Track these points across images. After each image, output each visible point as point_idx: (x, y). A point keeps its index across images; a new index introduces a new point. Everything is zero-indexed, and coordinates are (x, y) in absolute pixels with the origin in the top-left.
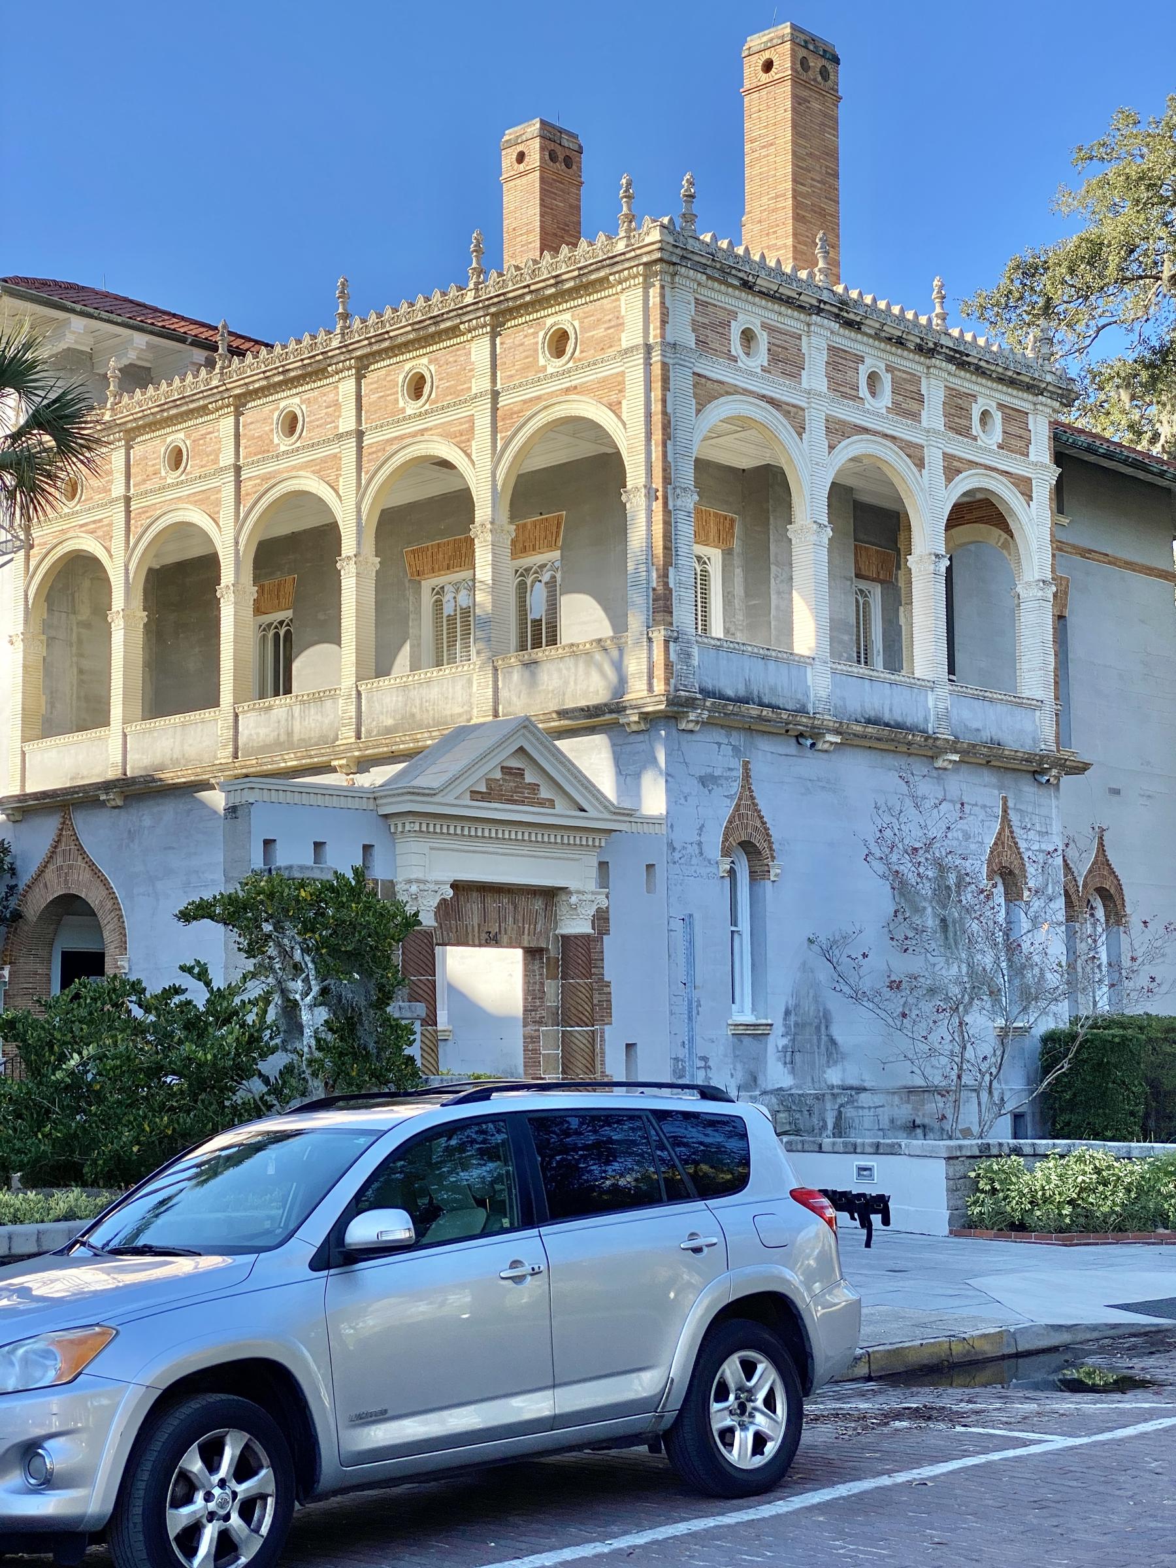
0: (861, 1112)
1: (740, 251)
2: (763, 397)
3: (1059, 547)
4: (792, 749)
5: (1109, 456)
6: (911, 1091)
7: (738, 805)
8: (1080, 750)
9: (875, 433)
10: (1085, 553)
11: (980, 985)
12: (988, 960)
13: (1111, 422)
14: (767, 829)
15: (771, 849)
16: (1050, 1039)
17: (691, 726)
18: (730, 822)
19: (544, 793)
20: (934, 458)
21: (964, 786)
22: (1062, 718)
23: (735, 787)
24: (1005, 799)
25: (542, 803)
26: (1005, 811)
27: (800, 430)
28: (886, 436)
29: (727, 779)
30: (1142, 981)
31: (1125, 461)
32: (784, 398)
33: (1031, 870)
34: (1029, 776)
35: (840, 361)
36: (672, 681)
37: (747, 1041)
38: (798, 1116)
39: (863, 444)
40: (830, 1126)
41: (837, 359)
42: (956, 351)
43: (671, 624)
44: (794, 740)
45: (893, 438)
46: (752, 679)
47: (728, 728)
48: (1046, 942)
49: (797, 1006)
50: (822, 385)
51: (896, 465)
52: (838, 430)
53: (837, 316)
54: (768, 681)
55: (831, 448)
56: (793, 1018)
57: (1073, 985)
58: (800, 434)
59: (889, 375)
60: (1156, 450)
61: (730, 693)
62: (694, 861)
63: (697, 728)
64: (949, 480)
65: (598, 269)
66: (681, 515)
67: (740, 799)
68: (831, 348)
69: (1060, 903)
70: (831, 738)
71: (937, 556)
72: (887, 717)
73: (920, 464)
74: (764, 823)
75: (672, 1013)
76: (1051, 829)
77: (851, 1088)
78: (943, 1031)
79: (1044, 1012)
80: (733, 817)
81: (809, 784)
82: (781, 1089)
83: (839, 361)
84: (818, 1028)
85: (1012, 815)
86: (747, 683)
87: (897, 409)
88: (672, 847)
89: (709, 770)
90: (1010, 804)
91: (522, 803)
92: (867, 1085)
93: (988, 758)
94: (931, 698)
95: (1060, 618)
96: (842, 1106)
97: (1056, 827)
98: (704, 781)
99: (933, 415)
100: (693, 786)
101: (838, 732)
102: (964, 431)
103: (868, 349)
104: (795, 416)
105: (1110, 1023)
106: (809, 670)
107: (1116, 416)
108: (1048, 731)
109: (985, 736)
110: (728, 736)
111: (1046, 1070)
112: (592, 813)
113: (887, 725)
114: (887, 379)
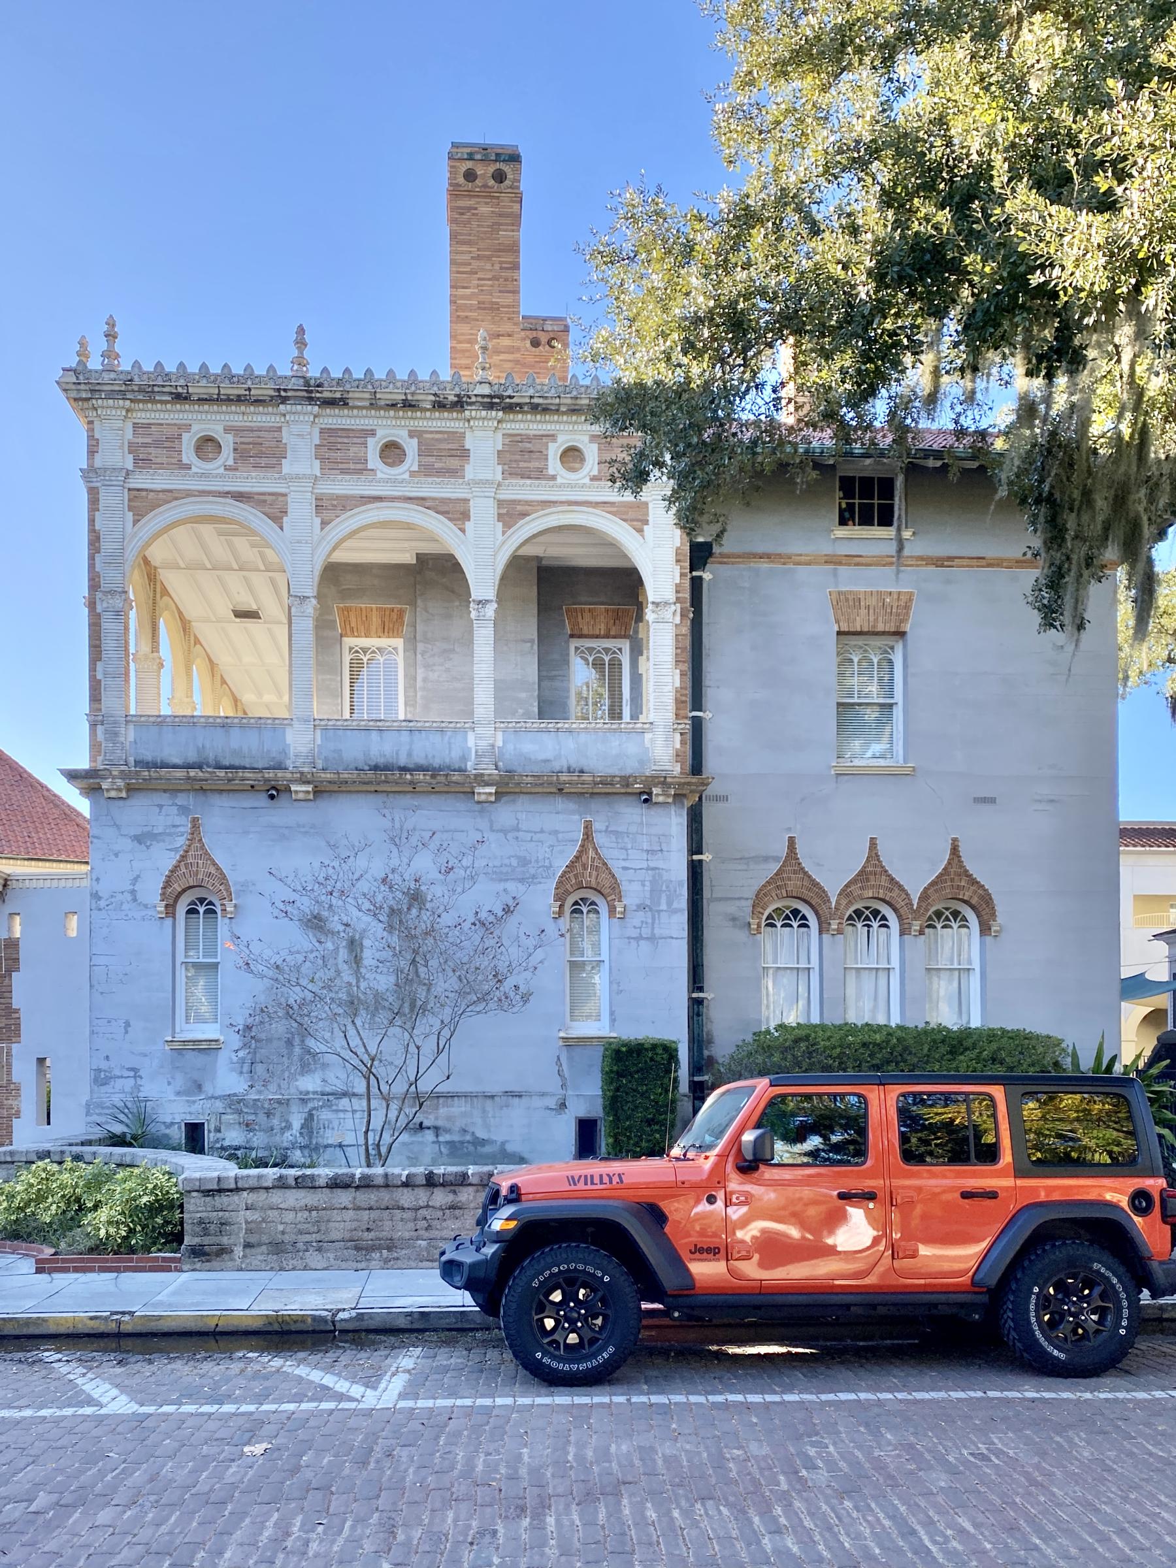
14: (222, 873)
17: (113, 794)
23: (181, 841)
29: (170, 834)
35: (340, 440)
39: (375, 513)
41: (332, 440)
46: (208, 745)
47: (174, 791)
55: (324, 523)
63: (124, 795)
74: (218, 869)
80: (176, 867)
84: (289, 1043)
89: (149, 828)
100: (128, 844)
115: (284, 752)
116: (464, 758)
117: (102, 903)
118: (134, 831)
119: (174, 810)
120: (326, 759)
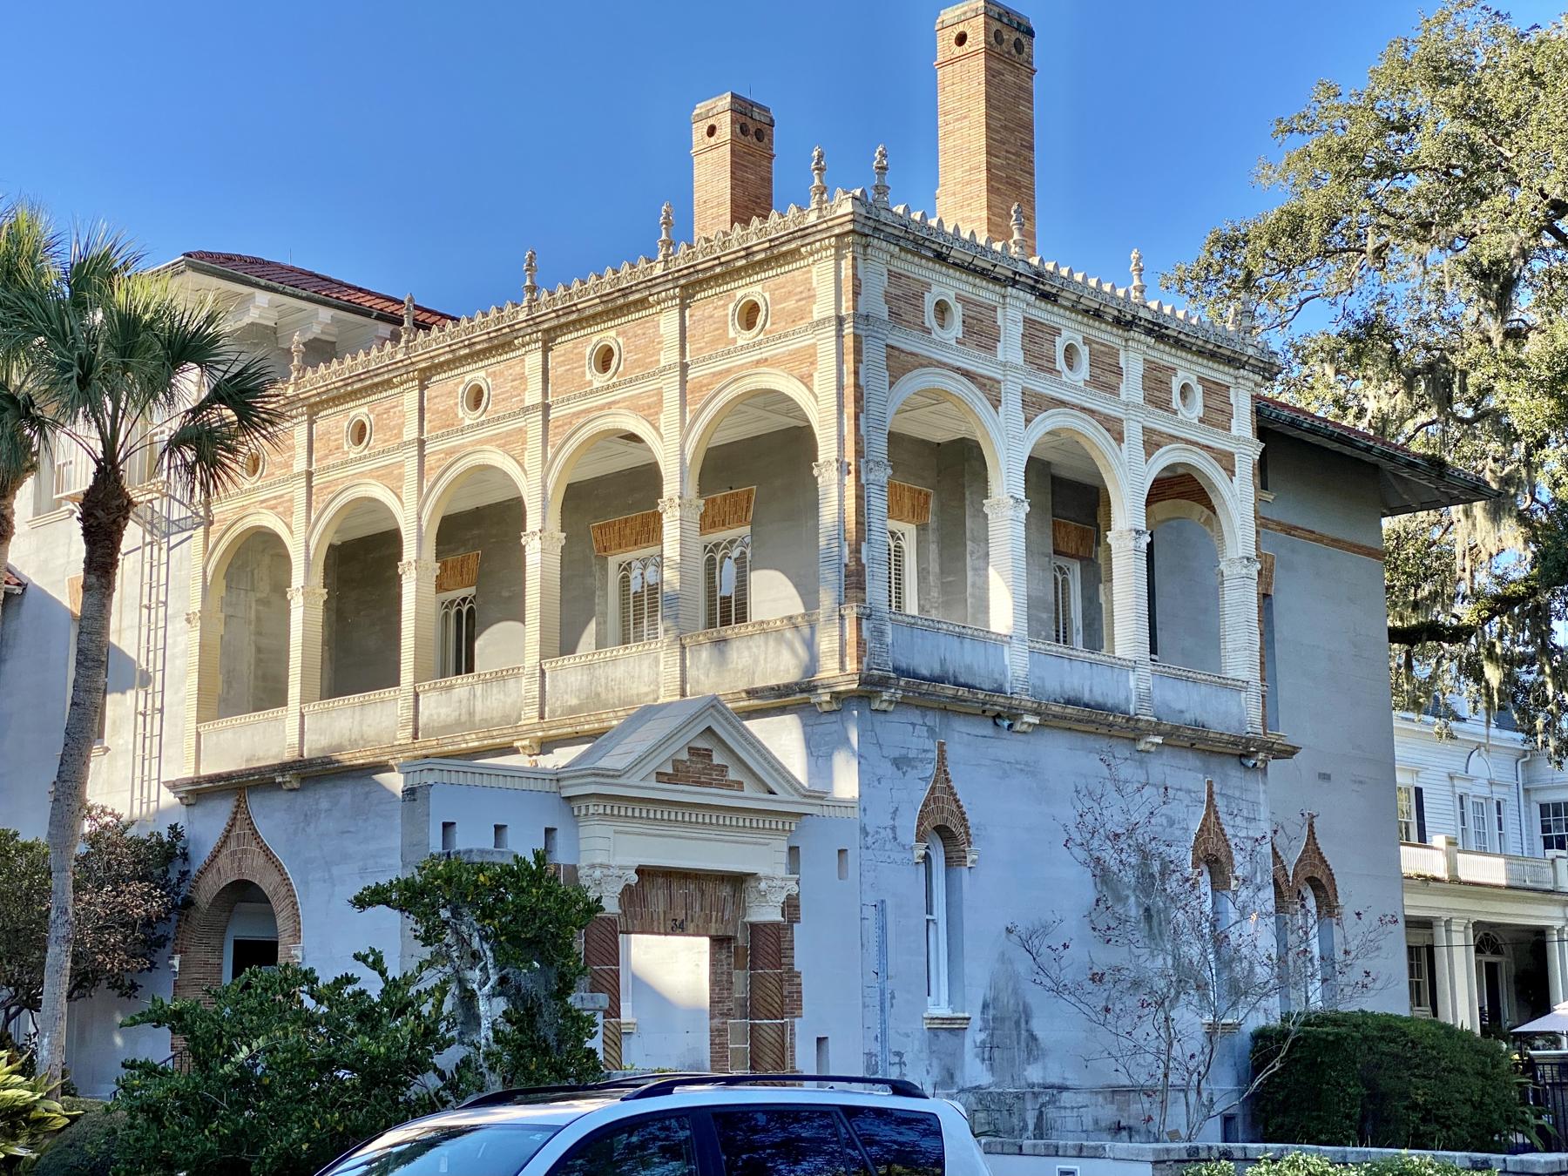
0: (1063, 1113)
1: (933, 222)
2: (958, 370)
3: (1262, 523)
4: (988, 730)
5: (1313, 430)
6: (1115, 1091)
7: (933, 789)
8: (1286, 734)
9: (1073, 406)
10: (1289, 530)
11: (1185, 978)
12: (1193, 952)
13: (1316, 394)
15: (967, 833)
16: (1261, 1036)
17: (884, 706)
18: (925, 805)
19: (732, 775)
20: (1133, 432)
21: (1168, 770)
22: (1268, 701)
23: (930, 770)
24: (1210, 784)
25: (730, 785)
26: (1210, 795)
27: (996, 403)
28: (1083, 409)
30: (1356, 975)
31: (1331, 436)
32: (980, 371)
33: (1238, 858)
34: (1235, 760)
36: (865, 660)
37: (943, 1035)
38: (997, 1115)
39: (1060, 418)
40: (1031, 1127)
42: (1154, 324)
43: (864, 601)
44: (991, 722)
45: (1092, 412)
47: (924, 709)
48: (1255, 934)
49: (995, 999)
50: (1017, 357)
51: (1095, 440)
52: (1034, 404)
53: (1033, 288)
54: (965, 659)
55: (1028, 421)
56: (991, 1012)
57: (1284, 982)
58: (996, 408)
59: (1087, 348)
60: (1362, 425)
61: (925, 672)
62: (888, 846)
64: (1149, 454)
65: (789, 241)
66: (874, 489)
67: (935, 782)
68: (1026, 320)
69: (1269, 893)
70: (1028, 719)
71: (1137, 532)
72: (1086, 697)
73: (1119, 438)
74: (959, 807)
75: (865, 1006)
76: (1260, 813)
77: (1052, 1087)
78: (1147, 1030)
79: (1254, 1007)
80: (927, 800)
81: (1007, 766)
82: (978, 1087)
83: (1035, 333)
84: (1017, 1023)
85: (1218, 800)
86: (943, 662)
87: (1094, 382)
88: (864, 832)
89: (904, 752)
90: (1216, 788)
91: (709, 785)
92: (1068, 1083)
93: (1192, 741)
94: (1132, 677)
95: (1265, 598)
96: (1043, 1105)
97: (1264, 813)
98: (900, 763)
99: (1132, 387)
100: (887, 769)
101: (1036, 713)
102: (1164, 405)
103: (1064, 322)
104: (990, 388)
105: (1323, 1020)
106: (1006, 649)
107: (1320, 389)
108: (1254, 713)
109: (1189, 717)
110: (924, 717)
111: (1257, 1070)
112: (781, 795)
113: (1087, 706)
114: (1084, 351)
115: (1004, 673)
116: (1128, 700)
117: (870, 840)
118: (896, 753)
119: (924, 731)
120: (1034, 687)
